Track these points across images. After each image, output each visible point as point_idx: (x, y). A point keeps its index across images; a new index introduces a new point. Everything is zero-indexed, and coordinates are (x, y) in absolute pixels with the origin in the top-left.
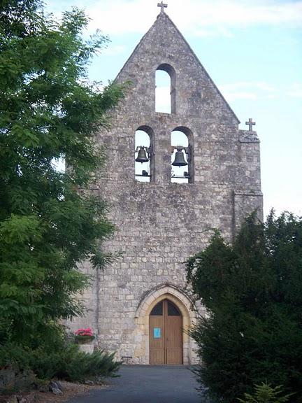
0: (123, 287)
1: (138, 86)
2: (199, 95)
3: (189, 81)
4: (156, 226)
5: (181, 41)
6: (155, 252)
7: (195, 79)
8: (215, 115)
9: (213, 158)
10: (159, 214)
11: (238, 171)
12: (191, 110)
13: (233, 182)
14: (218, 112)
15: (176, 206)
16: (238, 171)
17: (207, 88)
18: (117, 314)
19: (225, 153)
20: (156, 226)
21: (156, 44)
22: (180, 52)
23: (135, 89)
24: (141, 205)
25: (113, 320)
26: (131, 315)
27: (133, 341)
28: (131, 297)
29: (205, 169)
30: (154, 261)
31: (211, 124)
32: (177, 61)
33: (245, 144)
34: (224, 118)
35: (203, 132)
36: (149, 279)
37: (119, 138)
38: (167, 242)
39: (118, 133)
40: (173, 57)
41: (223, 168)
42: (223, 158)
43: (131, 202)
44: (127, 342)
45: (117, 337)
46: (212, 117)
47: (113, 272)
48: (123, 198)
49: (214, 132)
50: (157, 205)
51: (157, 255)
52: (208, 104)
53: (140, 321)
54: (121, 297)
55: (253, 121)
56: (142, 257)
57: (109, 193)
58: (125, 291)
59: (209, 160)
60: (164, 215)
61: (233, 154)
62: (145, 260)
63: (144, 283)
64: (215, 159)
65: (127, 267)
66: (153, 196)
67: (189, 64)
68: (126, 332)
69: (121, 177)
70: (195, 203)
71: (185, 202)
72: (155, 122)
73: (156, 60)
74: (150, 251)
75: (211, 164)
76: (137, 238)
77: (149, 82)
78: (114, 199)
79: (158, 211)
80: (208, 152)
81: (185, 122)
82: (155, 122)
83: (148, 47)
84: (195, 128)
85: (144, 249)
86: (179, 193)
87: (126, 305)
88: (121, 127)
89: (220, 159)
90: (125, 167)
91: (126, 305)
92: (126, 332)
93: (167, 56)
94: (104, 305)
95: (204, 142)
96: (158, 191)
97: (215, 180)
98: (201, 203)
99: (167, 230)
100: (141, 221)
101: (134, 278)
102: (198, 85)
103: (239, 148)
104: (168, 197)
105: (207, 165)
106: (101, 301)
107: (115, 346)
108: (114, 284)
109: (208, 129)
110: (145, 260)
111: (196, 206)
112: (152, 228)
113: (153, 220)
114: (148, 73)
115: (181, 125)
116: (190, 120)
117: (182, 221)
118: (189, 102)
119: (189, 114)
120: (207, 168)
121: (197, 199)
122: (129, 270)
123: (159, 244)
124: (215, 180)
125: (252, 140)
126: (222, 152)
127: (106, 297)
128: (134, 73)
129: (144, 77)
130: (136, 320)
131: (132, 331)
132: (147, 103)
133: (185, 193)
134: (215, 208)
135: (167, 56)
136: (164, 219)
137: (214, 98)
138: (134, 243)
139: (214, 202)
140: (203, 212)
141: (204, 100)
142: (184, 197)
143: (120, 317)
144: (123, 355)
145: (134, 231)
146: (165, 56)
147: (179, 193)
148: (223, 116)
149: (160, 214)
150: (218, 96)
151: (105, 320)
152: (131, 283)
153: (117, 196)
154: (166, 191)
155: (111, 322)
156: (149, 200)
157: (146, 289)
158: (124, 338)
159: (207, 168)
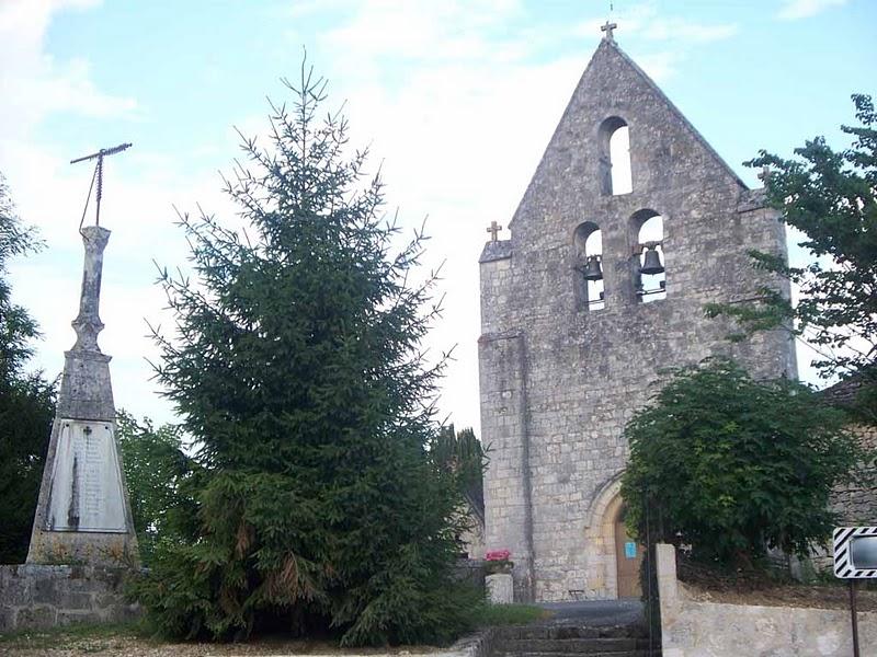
0: (564, 481)
1: (572, 164)
2: (667, 151)
3: (649, 133)
4: (609, 378)
5: (632, 75)
6: (609, 420)
7: (659, 128)
8: (694, 178)
9: (694, 250)
10: (612, 358)
11: (738, 261)
12: (657, 179)
13: (730, 282)
14: (701, 171)
15: (638, 341)
16: (738, 261)
17: (677, 137)
18: (558, 525)
19: (715, 237)
20: (609, 378)
21: (596, 90)
22: (632, 92)
23: (568, 170)
24: (585, 349)
25: (554, 534)
26: (579, 525)
27: (585, 566)
28: (578, 496)
29: (682, 272)
30: (608, 434)
31: (689, 194)
32: (628, 108)
33: (747, 214)
34: (710, 178)
35: (677, 211)
36: (603, 464)
37: (548, 251)
38: (627, 401)
39: (547, 244)
40: (622, 104)
41: (711, 262)
42: (710, 246)
43: (571, 346)
44: (576, 567)
45: (562, 560)
46: (692, 182)
47: (549, 461)
48: (557, 343)
49: (695, 205)
50: (609, 345)
51: (613, 424)
52: (682, 162)
53: (593, 532)
54: (563, 498)
55: (490, 226)
56: (591, 431)
57: (537, 339)
58: (570, 487)
59: (688, 254)
60: (621, 358)
61: (728, 235)
62: (595, 435)
63: (596, 472)
64: (698, 250)
65: (569, 449)
66: (601, 332)
67: (647, 107)
68: (573, 552)
69: (555, 311)
70: (668, 329)
71: (653, 332)
72: (601, 213)
73: (598, 115)
74: (602, 419)
75: (692, 260)
76: (581, 401)
77: (588, 152)
78: (545, 346)
79: (611, 354)
80: (687, 241)
81: (646, 201)
82: (601, 213)
83: (583, 100)
84: (663, 207)
85: (594, 417)
86: (641, 319)
87: (570, 509)
88: (552, 234)
89: (706, 248)
90: (559, 293)
91: (570, 509)
92: (573, 552)
93: (613, 103)
94: (540, 513)
95: (678, 227)
96: (610, 323)
97: (700, 284)
98: (678, 328)
99: (626, 382)
100: (587, 375)
101: (580, 465)
102: (664, 136)
103: (738, 222)
104: (626, 328)
105: (684, 263)
106: (535, 508)
107: (560, 574)
108: (552, 479)
109: (685, 202)
110: (595, 435)
111: (671, 334)
112: (603, 383)
113: (604, 370)
114: (586, 140)
115: (640, 208)
116: (654, 196)
117: (650, 364)
118: (651, 168)
119: (652, 186)
120: (685, 268)
121: (672, 322)
122: (573, 454)
123: (615, 406)
124: (700, 284)
125: (494, 253)
126: (709, 237)
127: (543, 499)
128: (566, 145)
129: (581, 146)
130: (587, 531)
131: (581, 549)
132: (587, 186)
133: (652, 317)
134: (703, 332)
135: (613, 103)
136: (620, 365)
137: (691, 150)
138: (578, 411)
139: (699, 323)
140: (682, 342)
141: (676, 158)
142: (650, 323)
143: (564, 529)
144: (571, 588)
145: (576, 392)
146: (609, 105)
147: (641, 319)
148: (709, 175)
149: (614, 358)
150: (696, 145)
151: (543, 536)
152: (577, 474)
153: (550, 341)
154: (622, 320)
155: (551, 538)
156: (597, 339)
157: (600, 482)
158: (571, 561)
159: (685, 268)
